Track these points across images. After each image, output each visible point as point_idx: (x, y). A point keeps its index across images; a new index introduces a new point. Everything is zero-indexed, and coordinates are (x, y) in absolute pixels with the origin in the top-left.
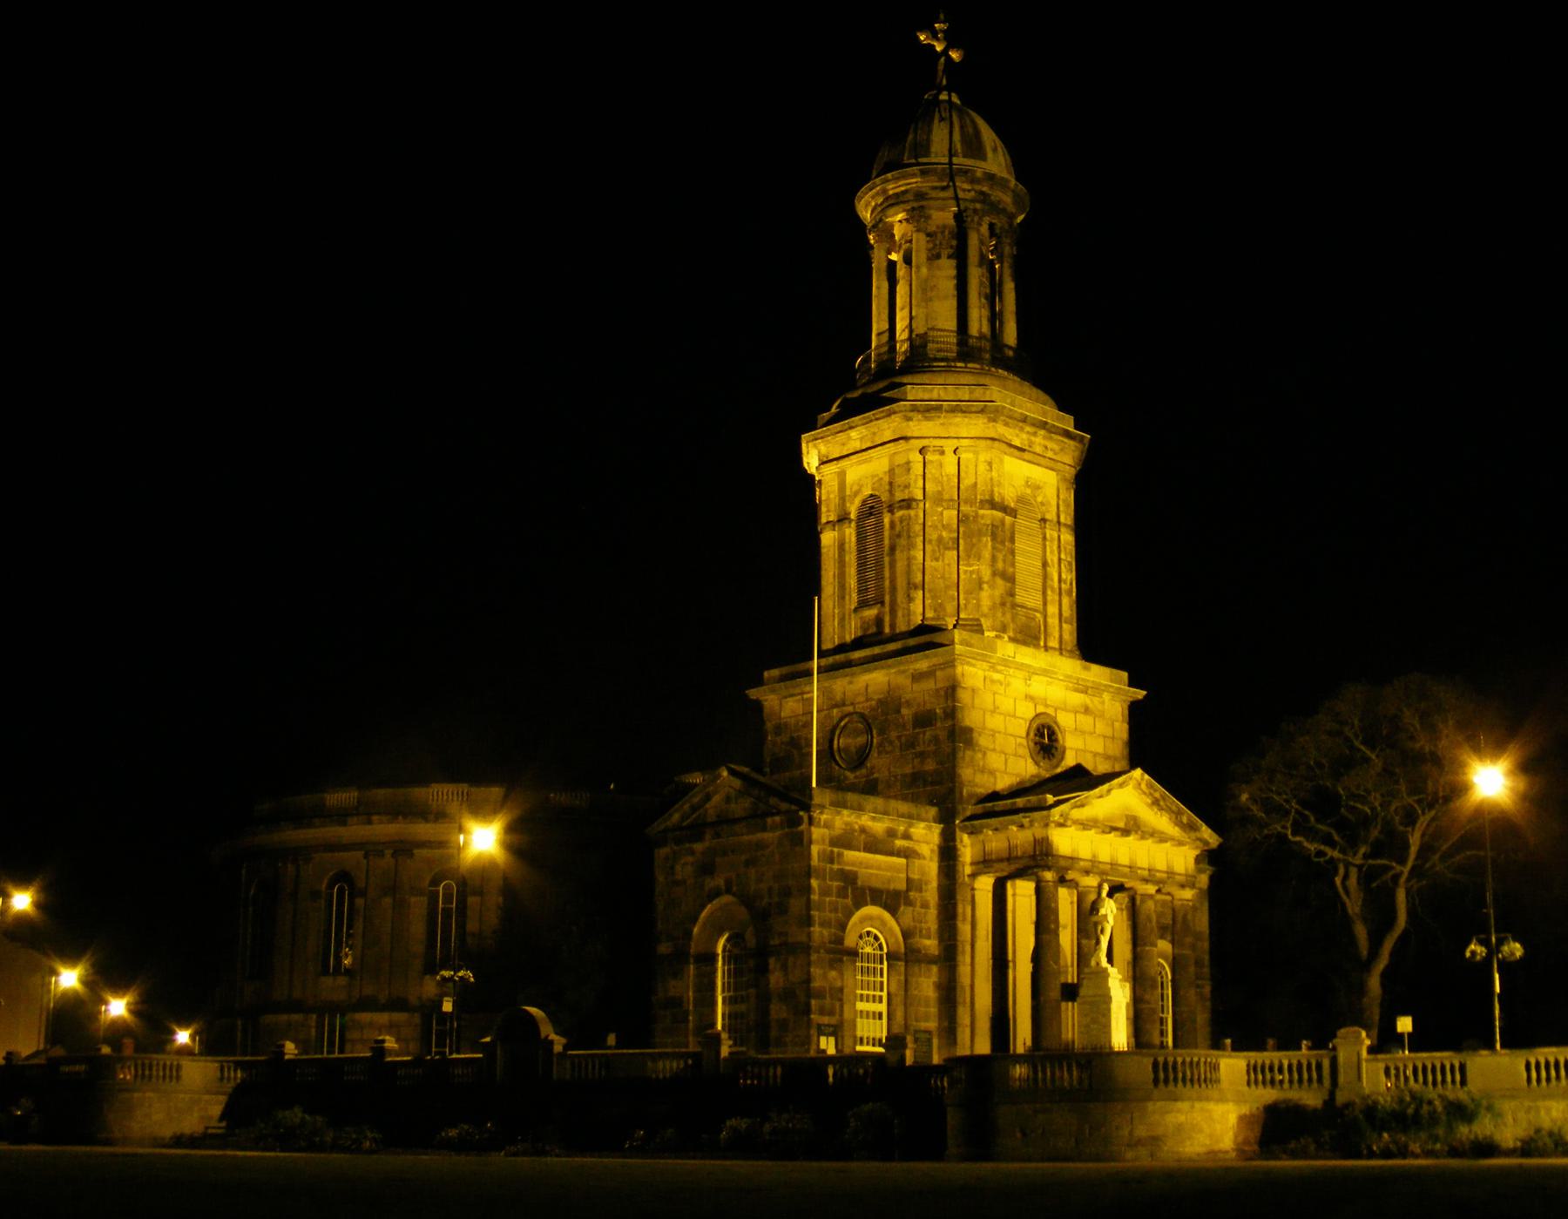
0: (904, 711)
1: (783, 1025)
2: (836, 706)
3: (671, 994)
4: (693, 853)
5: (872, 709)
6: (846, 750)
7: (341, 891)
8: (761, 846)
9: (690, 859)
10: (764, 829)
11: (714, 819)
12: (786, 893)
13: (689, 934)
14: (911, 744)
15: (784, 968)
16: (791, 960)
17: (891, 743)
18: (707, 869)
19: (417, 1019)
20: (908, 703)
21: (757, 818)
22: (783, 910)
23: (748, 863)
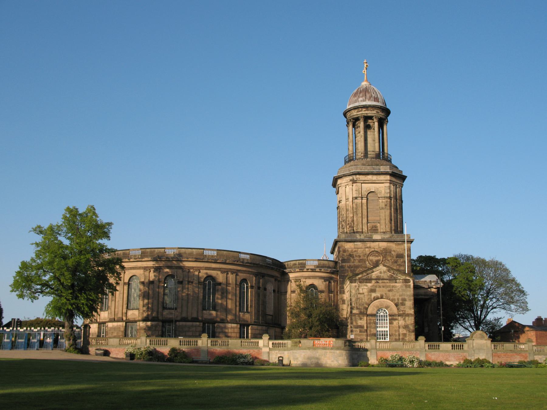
0: (393, 253)
1: (405, 335)
2: (368, 248)
3: (359, 324)
4: (367, 286)
5: (381, 251)
6: (371, 261)
7: (209, 283)
8: (393, 286)
9: (365, 287)
10: (396, 282)
11: (375, 277)
12: (404, 300)
13: (367, 309)
14: (396, 262)
15: (404, 319)
16: (407, 318)
17: (388, 260)
18: (373, 290)
19: (239, 326)
20: (394, 251)
21: (392, 279)
22: (403, 304)
23: (389, 291)
